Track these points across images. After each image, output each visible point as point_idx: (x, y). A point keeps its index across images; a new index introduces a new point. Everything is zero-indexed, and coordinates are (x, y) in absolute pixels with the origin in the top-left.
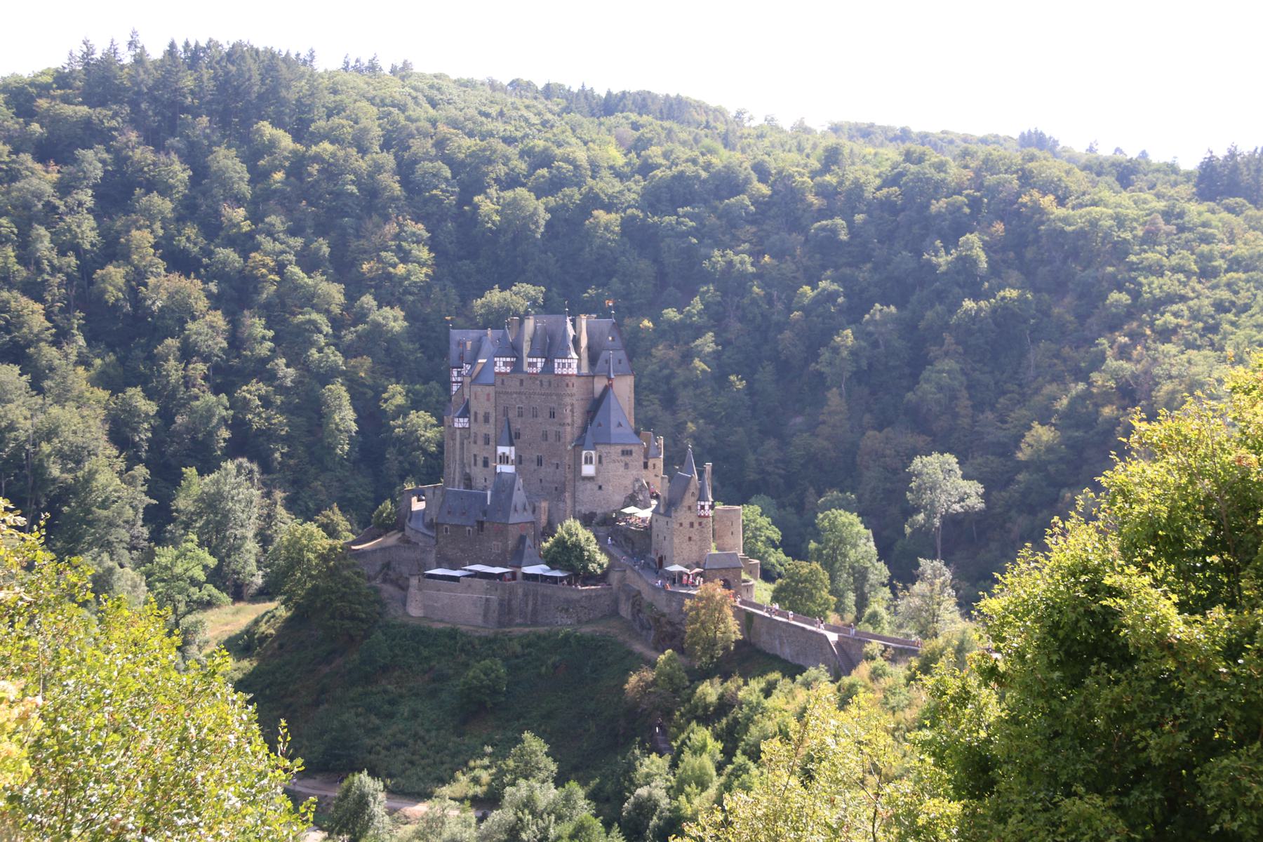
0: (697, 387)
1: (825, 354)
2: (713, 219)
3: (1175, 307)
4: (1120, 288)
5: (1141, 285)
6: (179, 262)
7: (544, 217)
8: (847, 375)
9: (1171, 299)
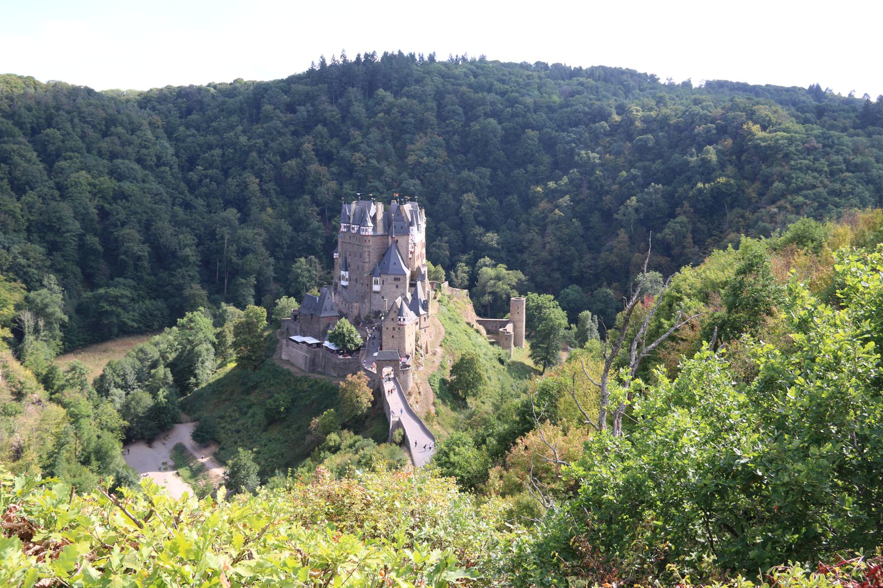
0: (558, 224)
2: (587, 135)
5: (792, 178)
6: (326, 158)
8: (632, 221)
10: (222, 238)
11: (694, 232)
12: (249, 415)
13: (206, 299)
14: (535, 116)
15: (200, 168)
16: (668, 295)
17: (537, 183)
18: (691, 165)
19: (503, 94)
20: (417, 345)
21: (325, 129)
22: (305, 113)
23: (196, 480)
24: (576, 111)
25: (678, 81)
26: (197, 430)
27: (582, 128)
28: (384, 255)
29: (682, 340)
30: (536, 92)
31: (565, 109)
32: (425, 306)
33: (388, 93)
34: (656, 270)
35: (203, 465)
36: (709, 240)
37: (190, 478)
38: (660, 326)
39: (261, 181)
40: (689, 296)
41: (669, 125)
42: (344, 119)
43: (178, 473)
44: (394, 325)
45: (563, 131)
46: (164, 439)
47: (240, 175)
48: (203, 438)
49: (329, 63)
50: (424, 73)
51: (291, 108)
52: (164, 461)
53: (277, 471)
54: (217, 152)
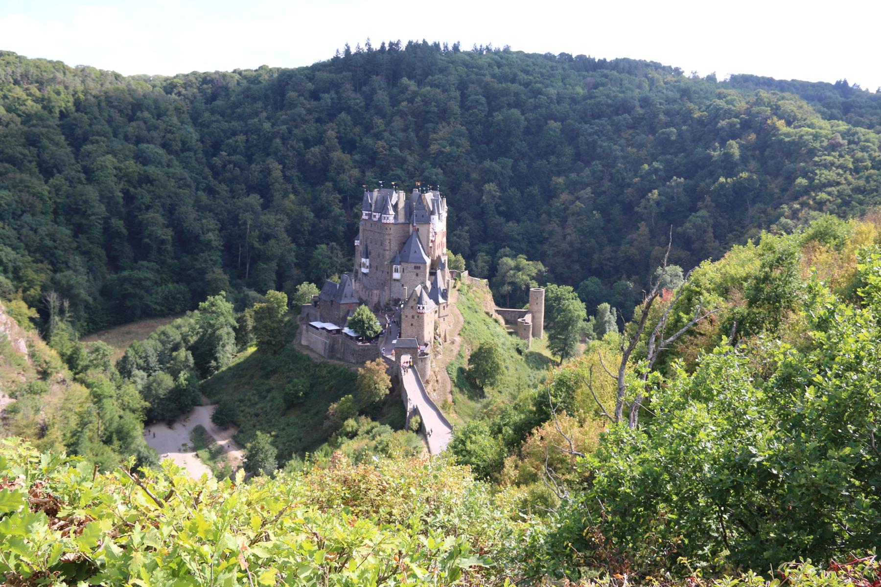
1: (643, 201)
3: (830, 189)
4: (805, 176)
5: (816, 174)
6: (349, 145)
7: (523, 123)
8: (653, 214)
9: (830, 184)
10: (245, 223)
11: (714, 226)
12: (268, 399)
13: (228, 283)
14: (559, 108)
15: (224, 153)
16: (688, 289)
17: (559, 174)
18: (714, 159)
19: (527, 85)
20: (436, 334)
21: (349, 117)
22: (329, 101)
23: (215, 463)
24: (599, 103)
25: (703, 75)
26: (217, 413)
27: (604, 120)
28: (404, 243)
29: (701, 334)
30: (560, 84)
31: (588, 101)
32: (445, 295)
33: (412, 82)
34: (676, 264)
35: (222, 447)
36: (730, 235)
37: (210, 459)
38: (679, 320)
39: (284, 167)
40: (708, 291)
41: (692, 118)
42: (367, 107)
43: (197, 455)
44: (414, 313)
45: (586, 123)
46: (185, 420)
47: (264, 161)
48: (222, 421)
49: (353, 51)
50: (448, 62)
51: (315, 95)
52: (184, 442)
53: (294, 455)
54: (241, 138)
